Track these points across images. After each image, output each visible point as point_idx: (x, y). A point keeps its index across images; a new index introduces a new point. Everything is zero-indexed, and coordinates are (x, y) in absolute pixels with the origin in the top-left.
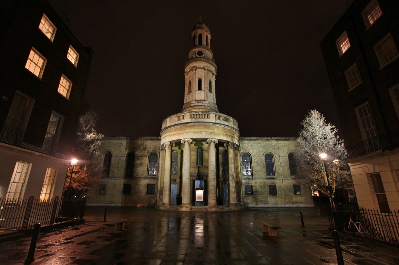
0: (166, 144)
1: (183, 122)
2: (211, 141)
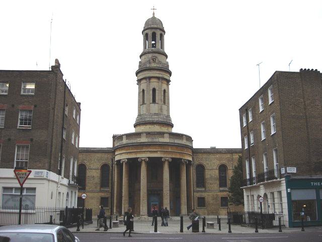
0: (124, 160)
1: (140, 141)
2: (166, 160)
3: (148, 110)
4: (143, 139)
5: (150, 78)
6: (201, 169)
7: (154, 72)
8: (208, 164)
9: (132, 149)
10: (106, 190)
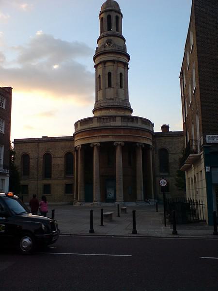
1: (92, 127)
3: (104, 95)
4: (95, 124)
5: (104, 62)
8: (171, 148)
9: (85, 135)
10: (70, 176)
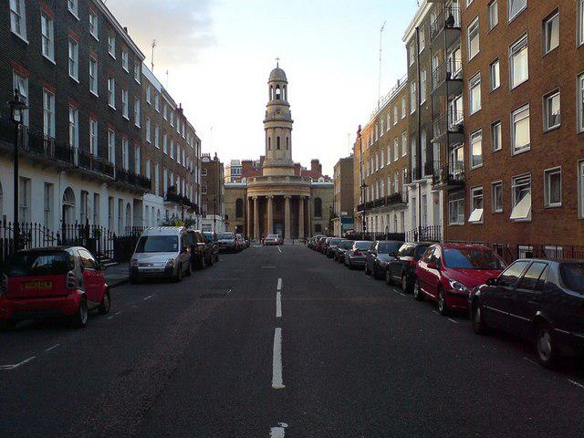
4: (270, 182)
5: (275, 128)
6: (318, 202)
7: (279, 120)
